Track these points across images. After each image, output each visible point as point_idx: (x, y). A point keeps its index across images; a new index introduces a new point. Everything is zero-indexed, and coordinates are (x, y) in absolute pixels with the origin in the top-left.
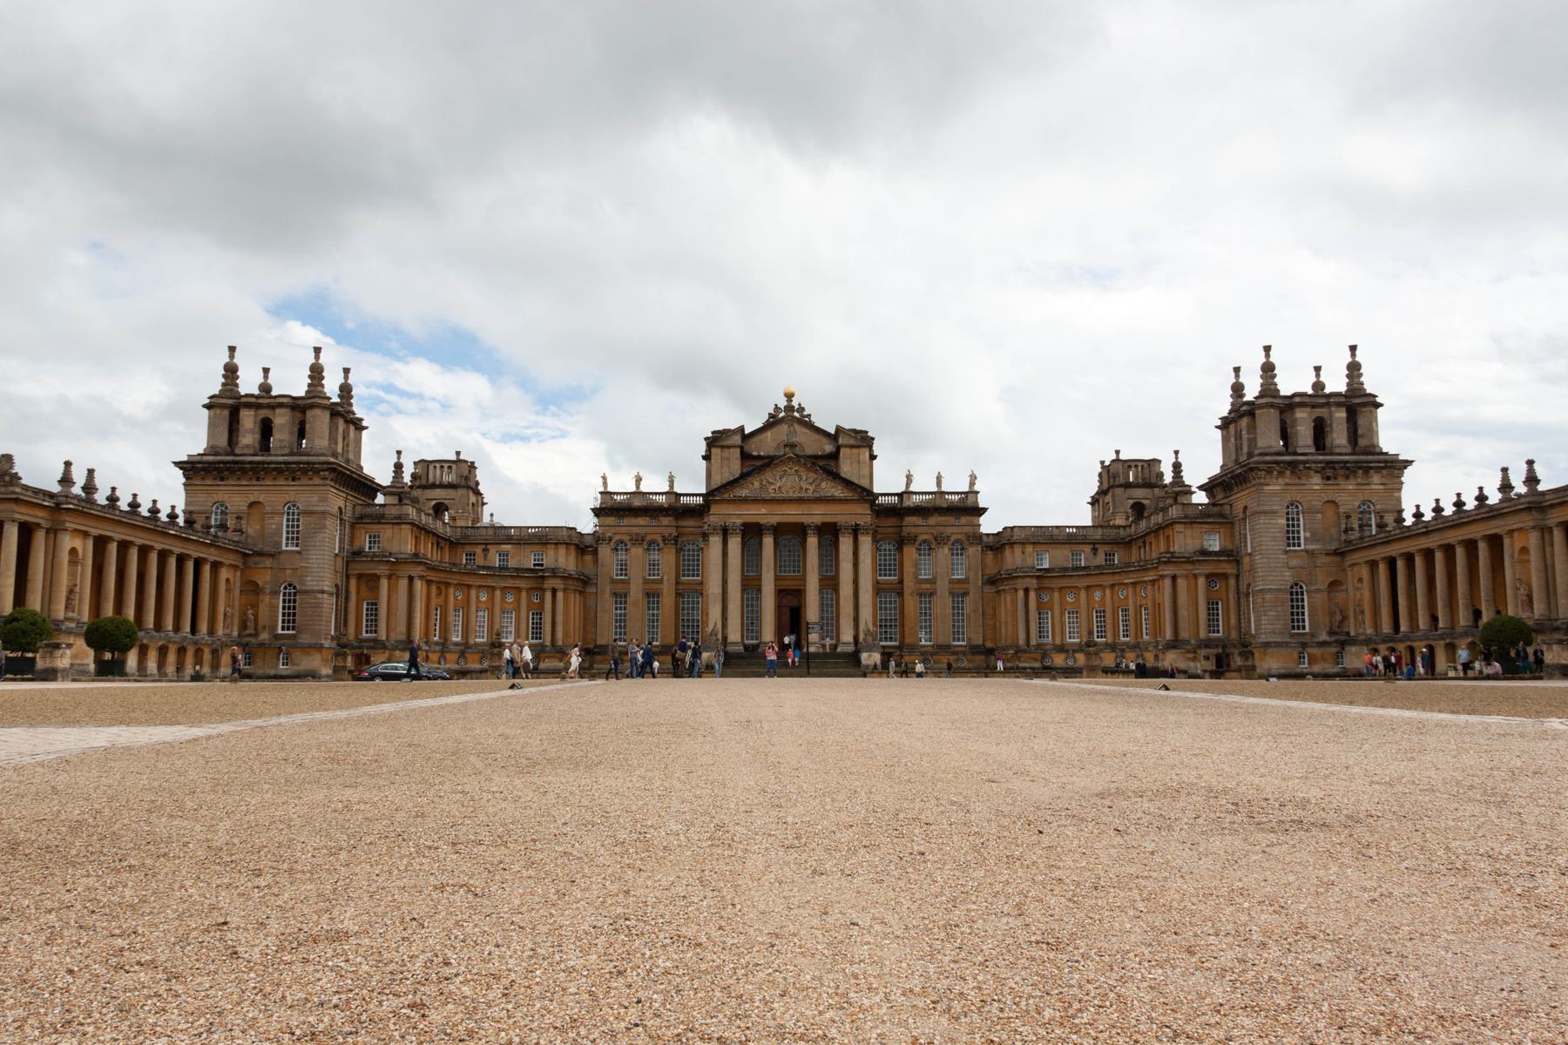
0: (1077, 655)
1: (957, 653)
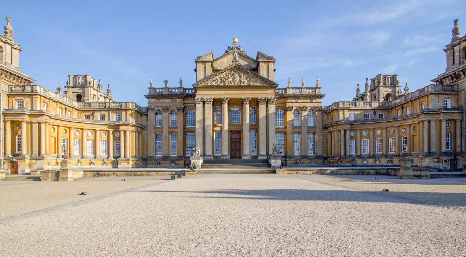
0: (368, 160)
1: (311, 159)
